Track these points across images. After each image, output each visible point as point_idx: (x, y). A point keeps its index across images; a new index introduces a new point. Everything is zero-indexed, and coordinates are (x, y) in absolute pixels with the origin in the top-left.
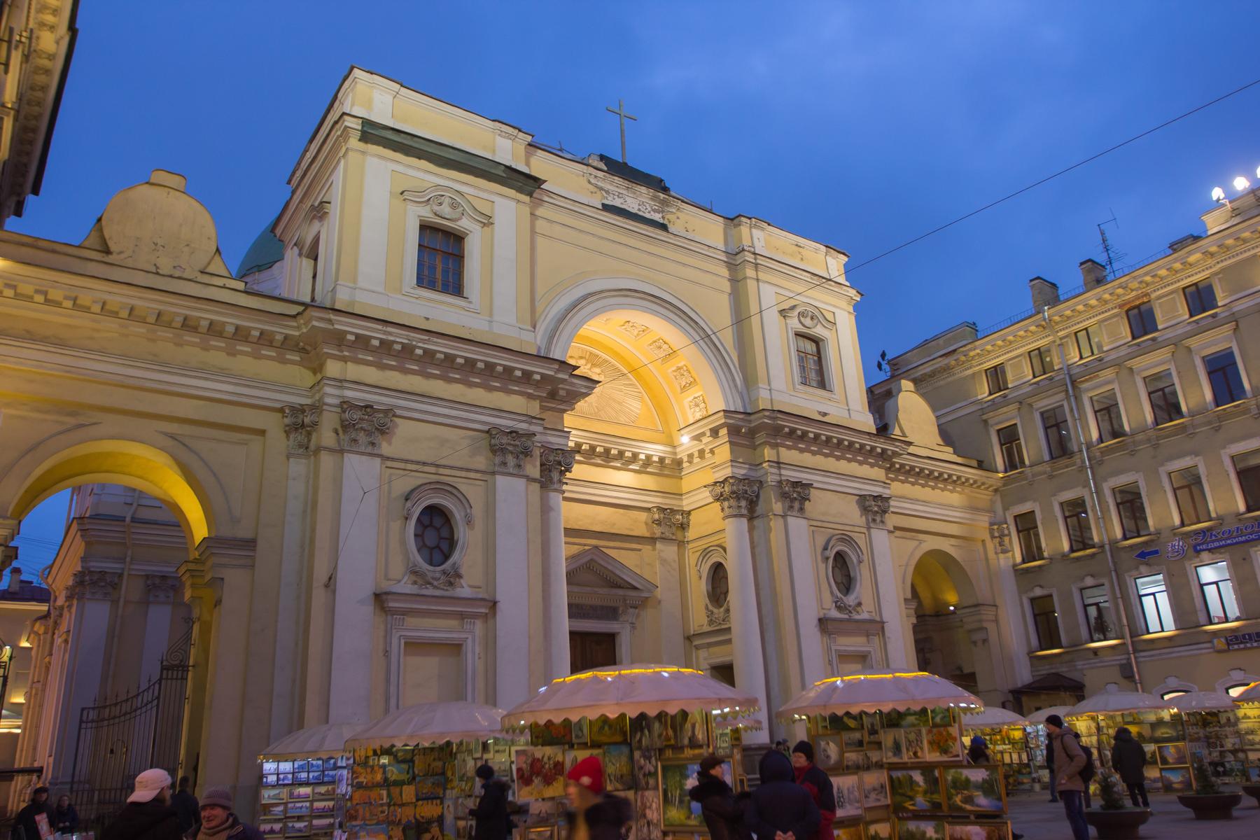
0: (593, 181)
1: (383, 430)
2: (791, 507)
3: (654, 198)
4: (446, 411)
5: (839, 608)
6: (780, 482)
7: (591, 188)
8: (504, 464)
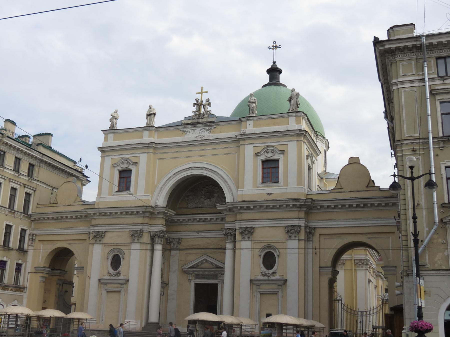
0: (181, 130)
1: (103, 237)
3: (206, 126)
5: (263, 275)
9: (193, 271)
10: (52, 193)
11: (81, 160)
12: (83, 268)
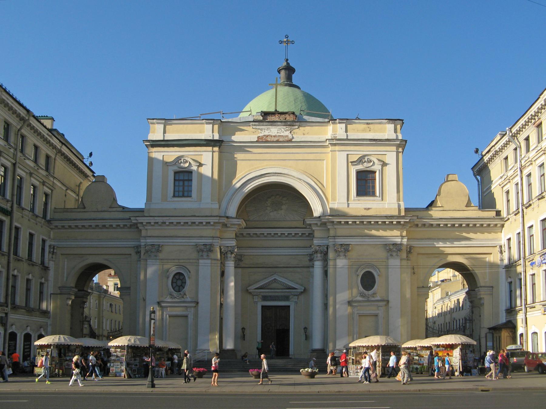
2: (339, 255)
3: (284, 125)
4: (181, 241)
6: (334, 245)
7: (254, 130)
8: (202, 256)
9: (261, 292)
10: (66, 195)
11: (91, 155)
12: (129, 288)
